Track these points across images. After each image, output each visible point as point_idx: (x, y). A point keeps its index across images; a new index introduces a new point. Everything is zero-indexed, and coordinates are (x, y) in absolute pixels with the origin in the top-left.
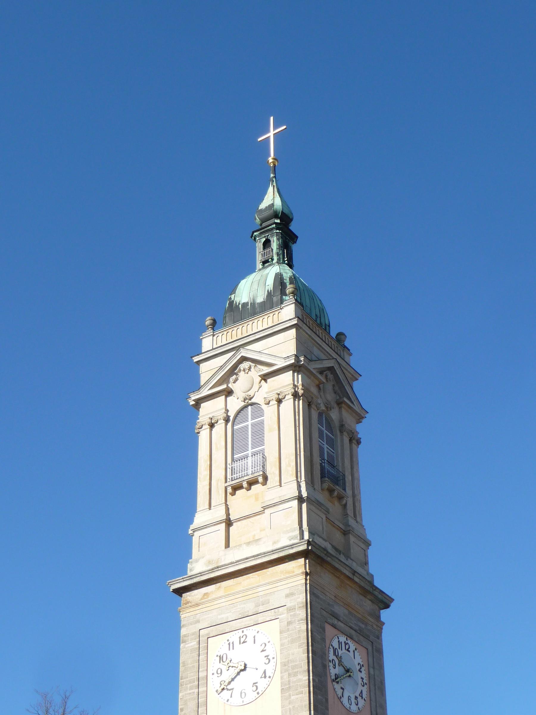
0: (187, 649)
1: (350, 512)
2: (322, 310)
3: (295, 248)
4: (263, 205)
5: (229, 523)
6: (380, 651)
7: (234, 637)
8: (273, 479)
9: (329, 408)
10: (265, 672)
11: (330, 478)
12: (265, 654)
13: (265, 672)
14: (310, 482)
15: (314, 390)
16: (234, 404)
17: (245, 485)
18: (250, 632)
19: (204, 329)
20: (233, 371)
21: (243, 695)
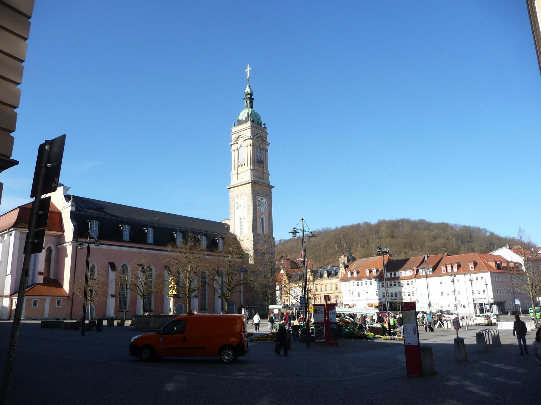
0: (231, 202)
1: (265, 169)
2: (260, 119)
3: (254, 102)
4: (246, 91)
5: (238, 174)
6: (271, 198)
7: (239, 198)
8: (246, 164)
9: (259, 145)
11: (260, 162)
14: (254, 165)
15: (255, 143)
16: (239, 146)
19: (232, 127)
20: (238, 138)
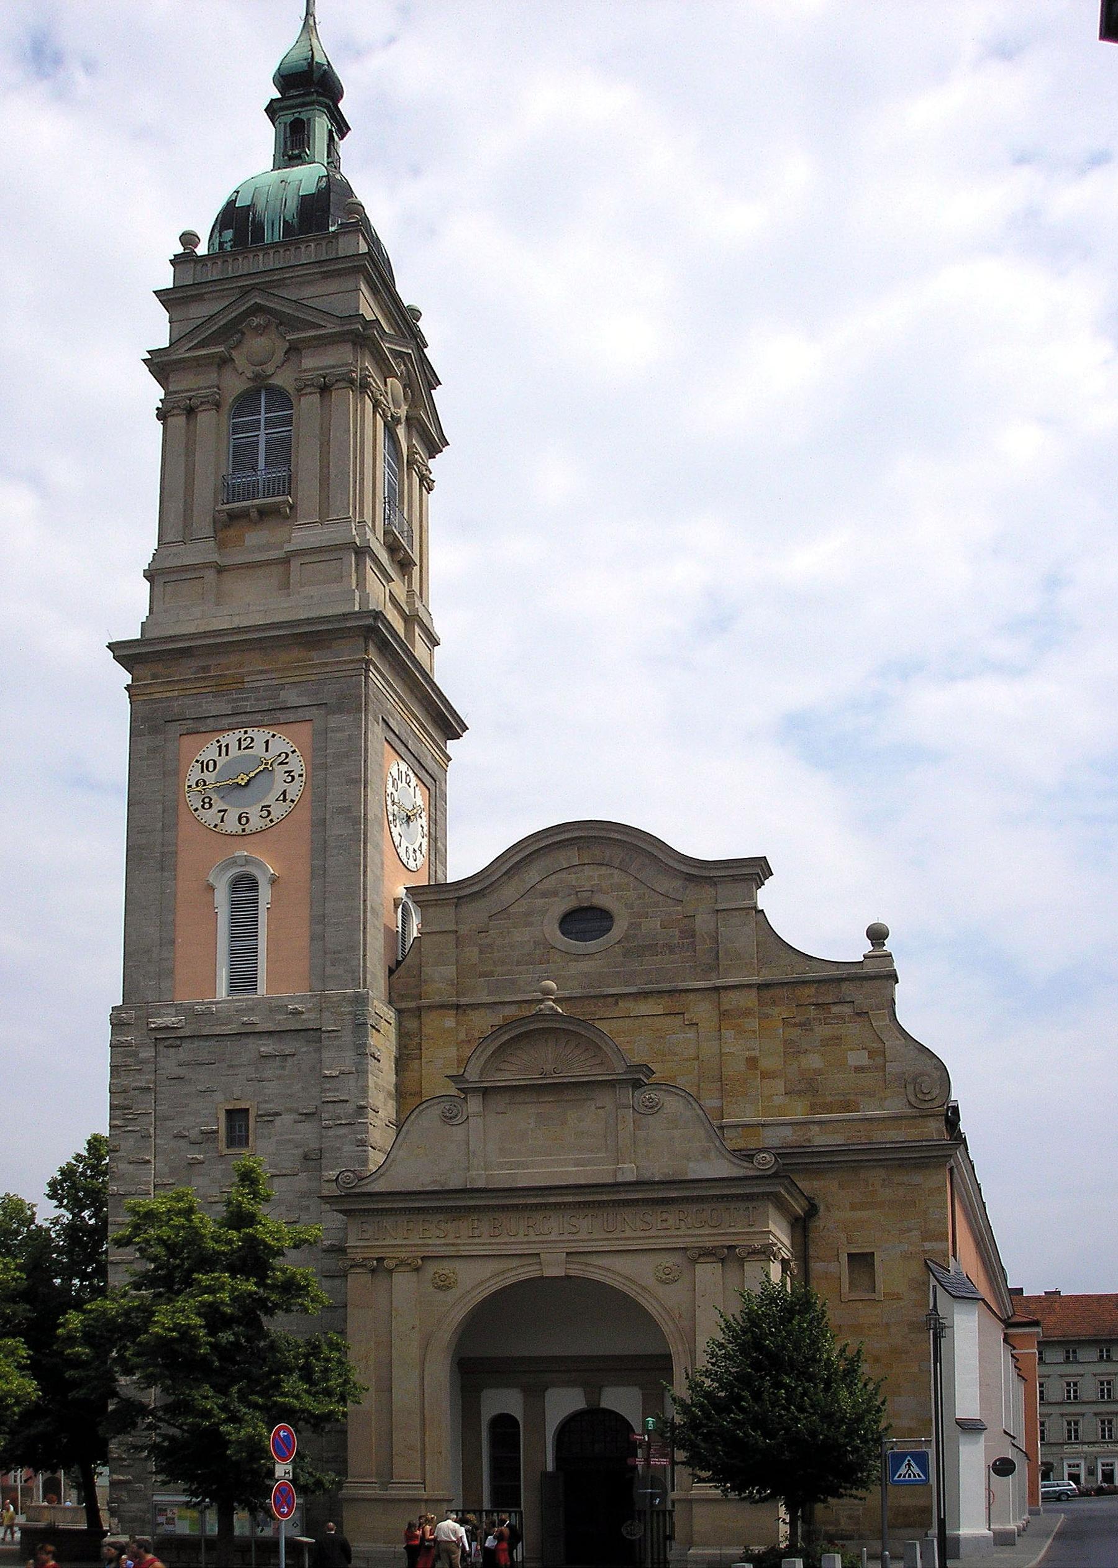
7: (230, 738)
10: (284, 793)
12: (286, 768)
13: (284, 793)
17: (254, 514)
18: (260, 735)
21: (244, 821)
